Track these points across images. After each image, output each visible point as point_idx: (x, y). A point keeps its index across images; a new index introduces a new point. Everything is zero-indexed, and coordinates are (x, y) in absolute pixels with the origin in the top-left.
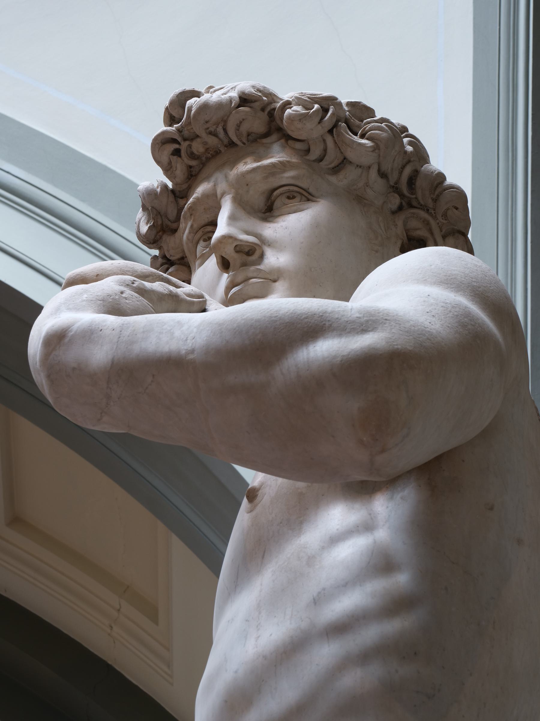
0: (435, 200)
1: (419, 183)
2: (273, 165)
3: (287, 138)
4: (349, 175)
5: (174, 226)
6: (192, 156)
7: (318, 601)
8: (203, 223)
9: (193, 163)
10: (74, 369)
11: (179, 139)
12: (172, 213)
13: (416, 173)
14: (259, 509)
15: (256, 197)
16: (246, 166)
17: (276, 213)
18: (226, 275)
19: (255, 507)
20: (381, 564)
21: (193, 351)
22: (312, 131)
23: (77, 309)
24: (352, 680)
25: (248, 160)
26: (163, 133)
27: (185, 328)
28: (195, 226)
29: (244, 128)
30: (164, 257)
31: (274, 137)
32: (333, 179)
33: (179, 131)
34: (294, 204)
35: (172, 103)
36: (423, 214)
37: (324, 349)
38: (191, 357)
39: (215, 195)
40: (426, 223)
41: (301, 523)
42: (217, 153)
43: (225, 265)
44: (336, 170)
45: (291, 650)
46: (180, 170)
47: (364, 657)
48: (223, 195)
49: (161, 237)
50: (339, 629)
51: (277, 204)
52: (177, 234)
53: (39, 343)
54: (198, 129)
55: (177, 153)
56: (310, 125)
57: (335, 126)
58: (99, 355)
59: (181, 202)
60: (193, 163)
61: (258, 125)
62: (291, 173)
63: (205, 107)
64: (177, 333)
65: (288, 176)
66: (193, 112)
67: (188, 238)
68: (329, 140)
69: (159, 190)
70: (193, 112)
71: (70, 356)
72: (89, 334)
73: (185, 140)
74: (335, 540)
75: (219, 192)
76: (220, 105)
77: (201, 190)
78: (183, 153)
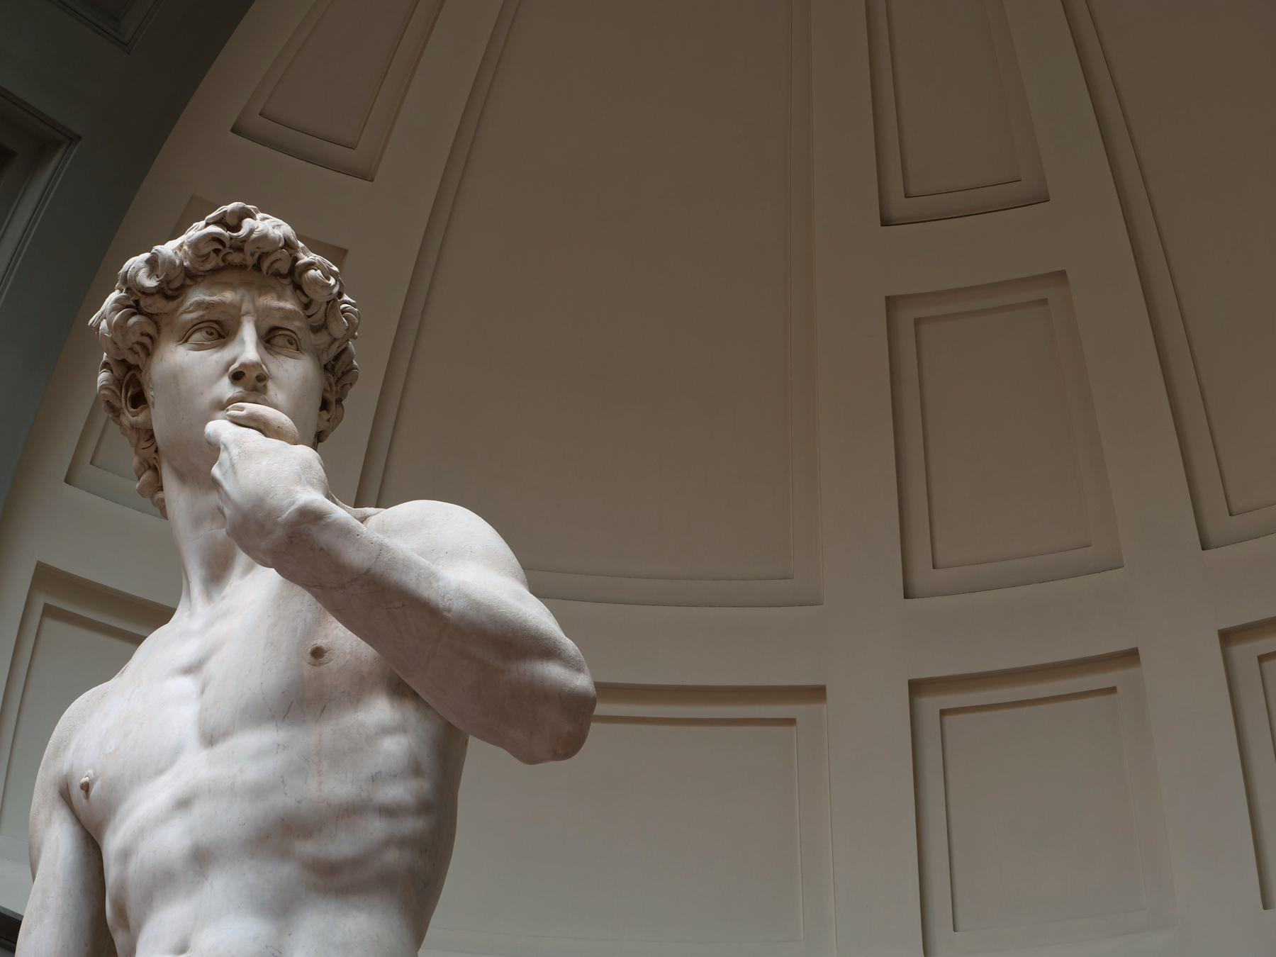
0: (345, 373)
1: (344, 357)
2: (290, 311)
3: (298, 287)
4: (323, 339)
5: (169, 293)
6: (224, 260)
7: (375, 779)
8: (213, 318)
9: (222, 264)
10: (322, 549)
11: (228, 244)
12: (176, 284)
13: (345, 349)
14: (323, 668)
15: (266, 324)
16: (270, 301)
17: (277, 349)
18: (226, 381)
19: (320, 664)
20: (415, 770)
21: (449, 611)
22: (321, 297)
23: (310, 483)
24: (392, 857)
25: (274, 295)
26: (221, 234)
27: (441, 584)
28: (206, 318)
29: (277, 265)
30: (137, 302)
31: (287, 281)
32: (312, 335)
33: (231, 238)
34: (292, 350)
35: (233, 212)
36: (332, 380)
37: (554, 671)
38: (447, 614)
39: (240, 309)
40: (331, 386)
41: (358, 700)
42: (242, 267)
43: (237, 377)
44: (316, 330)
45: (351, 811)
46: (209, 266)
47: (402, 842)
48: (247, 313)
49: (152, 294)
50: (388, 811)
51: (279, 341)
52: (172, 304)
53: (290, 506)
54: (248, 248)
55: (217, 251)
56: (326, 293)
57: (334, 300)
58: (355, 557)
59: (188, 282)
60: (222, 264)
61: (284, 267)
62: (297, 323)
63: (264, 237)
64: (435, 585)
65: (295, 325)
66: (254, 236)
67: (192, 320)
68: (324, 306)
69: (178, 262)
70: (254, 236)
71: (325, 538)
72: (344, 531)
73: (231, 247)
74: (385, 731)
75: (244, 308)
76: (274, 241)
77: (228, 296)
78: (221, 255)
